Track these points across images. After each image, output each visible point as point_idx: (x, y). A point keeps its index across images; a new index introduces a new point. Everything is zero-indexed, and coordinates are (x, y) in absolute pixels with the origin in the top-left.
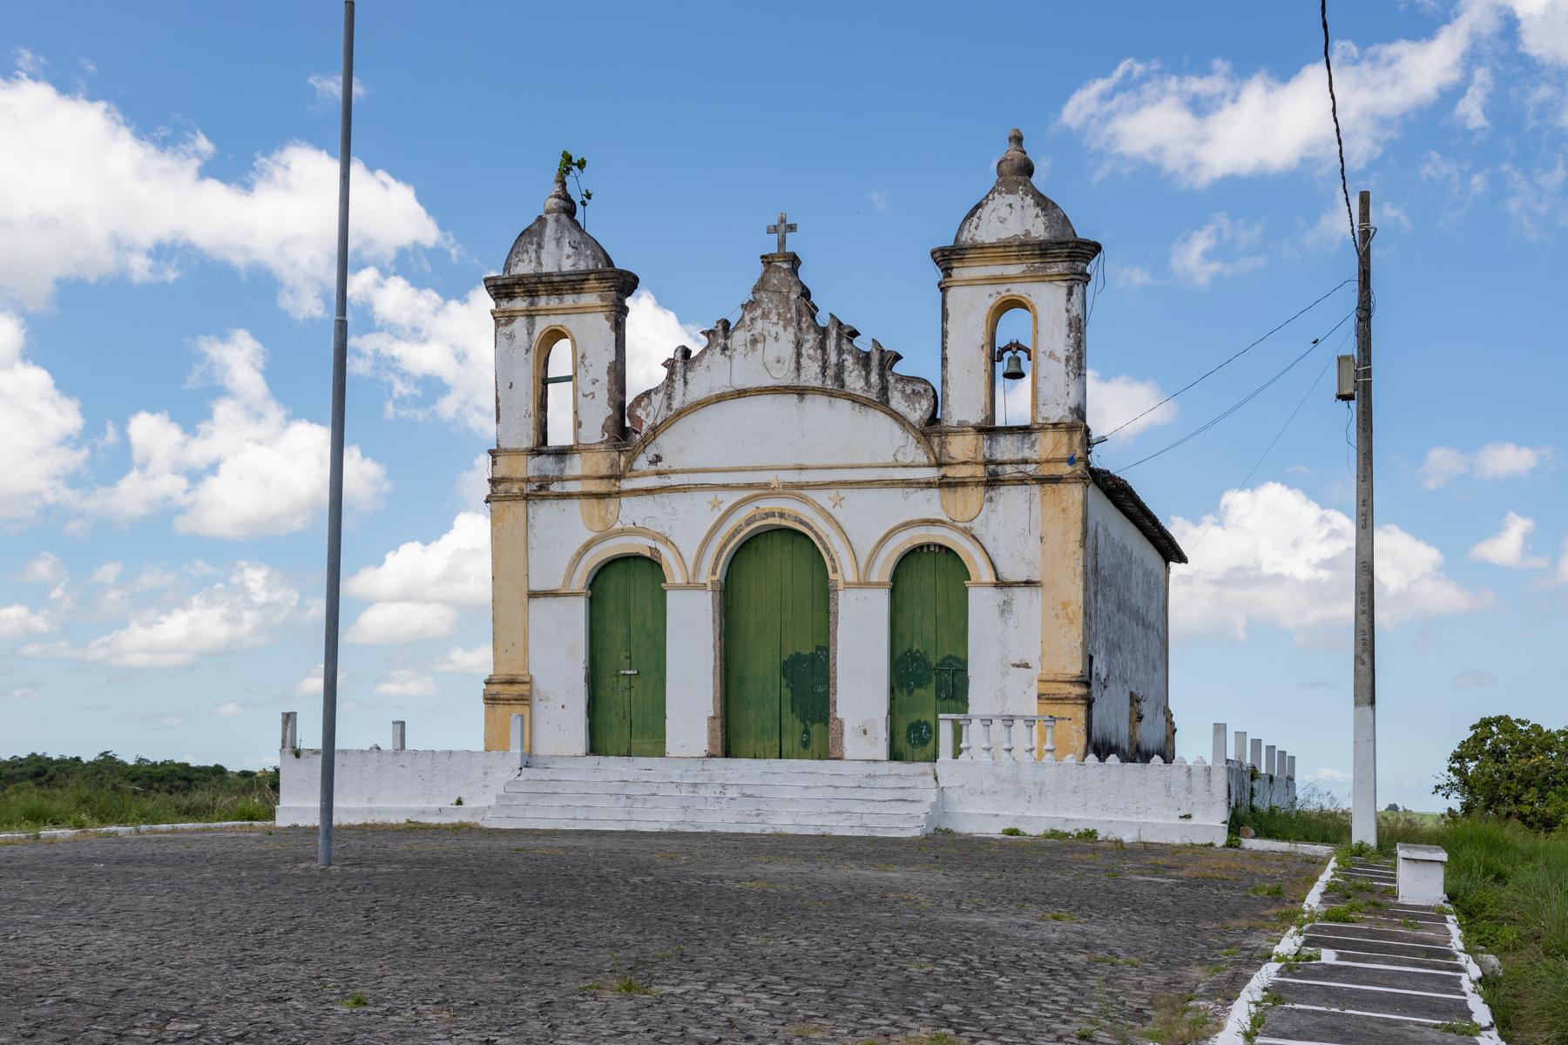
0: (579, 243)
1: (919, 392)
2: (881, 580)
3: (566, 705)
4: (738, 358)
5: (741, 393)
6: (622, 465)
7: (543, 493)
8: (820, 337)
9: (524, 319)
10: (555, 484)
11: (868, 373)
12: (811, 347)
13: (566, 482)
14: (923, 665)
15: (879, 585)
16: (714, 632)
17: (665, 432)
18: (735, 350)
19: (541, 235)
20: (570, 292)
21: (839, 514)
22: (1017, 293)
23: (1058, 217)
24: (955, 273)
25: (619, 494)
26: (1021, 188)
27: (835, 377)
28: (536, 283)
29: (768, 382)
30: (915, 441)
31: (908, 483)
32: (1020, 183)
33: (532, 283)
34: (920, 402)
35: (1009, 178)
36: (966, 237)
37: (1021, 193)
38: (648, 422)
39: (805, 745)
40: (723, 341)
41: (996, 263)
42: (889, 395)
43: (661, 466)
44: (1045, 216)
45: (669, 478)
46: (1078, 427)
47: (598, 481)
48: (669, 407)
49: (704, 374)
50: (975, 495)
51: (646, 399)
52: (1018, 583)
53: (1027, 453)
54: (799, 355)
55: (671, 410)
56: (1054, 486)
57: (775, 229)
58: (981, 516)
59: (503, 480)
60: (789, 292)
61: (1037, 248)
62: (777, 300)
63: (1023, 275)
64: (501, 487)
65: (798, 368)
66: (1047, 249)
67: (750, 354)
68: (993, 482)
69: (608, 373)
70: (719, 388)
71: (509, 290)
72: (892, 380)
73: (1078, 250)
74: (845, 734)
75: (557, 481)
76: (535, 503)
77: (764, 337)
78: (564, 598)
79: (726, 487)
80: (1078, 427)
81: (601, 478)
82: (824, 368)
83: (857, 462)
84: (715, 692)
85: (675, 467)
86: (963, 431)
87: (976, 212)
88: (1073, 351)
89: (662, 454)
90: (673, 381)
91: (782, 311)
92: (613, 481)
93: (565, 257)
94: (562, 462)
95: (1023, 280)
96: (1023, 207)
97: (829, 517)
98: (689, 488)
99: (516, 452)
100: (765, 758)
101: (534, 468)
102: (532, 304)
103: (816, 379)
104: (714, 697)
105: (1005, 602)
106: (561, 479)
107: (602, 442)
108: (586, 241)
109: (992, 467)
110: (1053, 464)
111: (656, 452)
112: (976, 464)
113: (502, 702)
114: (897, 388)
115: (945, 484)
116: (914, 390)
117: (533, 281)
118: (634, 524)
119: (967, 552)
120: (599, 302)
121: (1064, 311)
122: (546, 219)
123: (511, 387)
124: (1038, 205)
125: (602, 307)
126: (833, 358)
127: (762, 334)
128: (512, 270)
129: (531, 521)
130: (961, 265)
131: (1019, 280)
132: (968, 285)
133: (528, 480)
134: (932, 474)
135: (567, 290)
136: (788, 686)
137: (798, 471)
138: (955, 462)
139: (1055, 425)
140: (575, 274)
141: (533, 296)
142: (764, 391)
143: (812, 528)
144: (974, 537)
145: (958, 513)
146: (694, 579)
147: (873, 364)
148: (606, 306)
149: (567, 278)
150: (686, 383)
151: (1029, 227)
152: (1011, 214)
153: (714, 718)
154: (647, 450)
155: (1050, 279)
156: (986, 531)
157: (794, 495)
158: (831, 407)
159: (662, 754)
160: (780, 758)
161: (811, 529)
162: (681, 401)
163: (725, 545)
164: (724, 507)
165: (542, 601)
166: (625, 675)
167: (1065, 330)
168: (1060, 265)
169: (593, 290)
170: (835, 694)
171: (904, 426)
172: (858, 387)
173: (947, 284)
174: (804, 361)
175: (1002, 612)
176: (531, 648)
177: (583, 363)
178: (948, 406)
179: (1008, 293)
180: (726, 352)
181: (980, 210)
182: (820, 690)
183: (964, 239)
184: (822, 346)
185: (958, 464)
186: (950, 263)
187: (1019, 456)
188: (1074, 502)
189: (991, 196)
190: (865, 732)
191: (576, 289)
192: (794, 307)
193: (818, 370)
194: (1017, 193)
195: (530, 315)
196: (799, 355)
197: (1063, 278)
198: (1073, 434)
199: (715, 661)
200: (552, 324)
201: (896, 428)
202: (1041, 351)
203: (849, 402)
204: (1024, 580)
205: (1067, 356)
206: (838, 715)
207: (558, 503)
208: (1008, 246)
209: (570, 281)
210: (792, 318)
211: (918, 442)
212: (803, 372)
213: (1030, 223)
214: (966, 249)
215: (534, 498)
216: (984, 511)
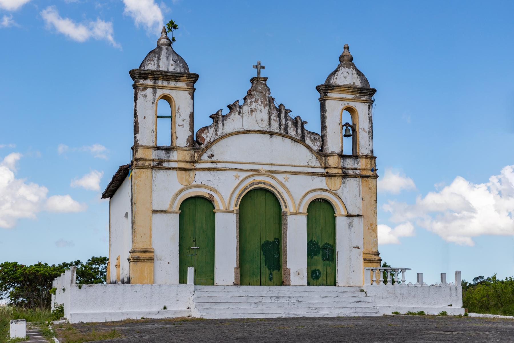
0: (177, 60)
1: (316, 138)
2: (304, 212)
3: (170, 263)
4: (245, 117)
5: (248, 132)
6: (196, 157)
7: (160, 166)
8: (278, 113)
9: (151, 89)
10: (165, 163)
11: (297, 129)
12: (275, 116)
13: (170, 163)
14: (317, 247)
15: (303, 214)
16: (237, 231)
17: (215, 145)
18: (244, 114)
19: (160, 54)
21: (287, 184)
22: (351, 105)
24: (329, 94)
25: (196, 169)
27: (284, 129)
28: (159, 75)
29: (257, 128)
30: (316, 158)
31: (314, 174)
32: (351, 65)
33: (157, 74)
34: (317, 142)
35: (347, 62)
36: (332, 81)
37: (351, 68)
38: (207, 140)
39: (271, 279)
40: (239, 109)
42: (305, 138)
43: (213, 159)
44: (360, 78)
45: (217, 164)
46: (374, 158)
47: (185, 163)
48: (216, 134)
49: (231, 122)
50: (339, 180)
51: (206, 130)
52: (355, 215)
53: (356, 166)
54: (270, 119)
55: (217, 136)
56: (366, 179)
57: (257, 67)
58: (340, 189)
59: (141, 159)
60: (266, 93)
61: (359, 90)
62: (261, 96)
63: (354, 99)
64: (140, 163)
65: (270, 124)
67: (250, 116)
68: (345, 176)
70: (237, 129)
72: (306, 133)
73: (372, 93)
74: (291, 275)
75: (167, 162)
76: (156, 171)
77: (256, 110)
78: (169, 214)
79: (242, 170)
80: (374, 158)
81: (187, 162)
82: (280, 125)
83: (293, 164)
84: (237, 257)
85: (219, 160)
86: (334, 156)
87: (336, 73)
88: (371, 129)
89: (214, 154)
90: (218, 124)
91: (263, 100)
92: (192, 164)
93: (170, 65)
94: (169, 153)
95: (353, 101)
96: (352, 73)
97: (283, 186)
98: (226, 169)
99: (148, 147)
100: (254, 285)
101: (155, 155)
103: (277, 129)
104: (237, 259)
105: (350, 222)
106: (168, 161)
107: (187, 147)
108: (179, 60)
109: (344, 170)
110: (366, 171)
111: (211, 153)
112: (339, 168)
113: (141, 261)
114: (308, 136)
115: (328, 175)
116: (314, 138)
117: (158, 74)
118: (202, 183)
119: (336, 202)
120: (185, 86)
121: (367, 114)
122: (162, 48)
123: (145, 118)
124: (357, 74)
125: (188, 89)
126: (284, 122)
127: (255, 109)
128: (145, 67)
129: (154, 179)
130: (331, 92)
131: (352, 101)
133: (153, 160)
134: (322, 171)
135: (172, 79)
136: (263, 255)
137: (271, 166)
138: (331, 167)
139: (366, 156)
140: (178, 73)
141: (156, 80)
142: (257, 132)
143: (276, 189)
144: (338, 196)
145: (332, 187)
146: (229, 208)
147: (299, 126)
149: (174, 74)
150: (223, 125)
151: (355, 81)
152: (348, 75)
153: (237, 268)
154: (207, 152)
155: (362, 102)
156: (343, 195)
157: (270, 175)
158: (283, 141)
159: (213, 284)
160: (261, 285)
161: (276, 189)
162: (221, 132)
163: (241, 194)
164: (241, 179)
165: (159, 215)
166: (193, 249)
167: (368, 121)
168: (366, 97)
169: (184, 81)
170: (286, 258)
171: (311, 152)
172: (293, 134)
173: (326, 98)
174: (272, 121)
175: (349, 227)
176: (153, 236)
177: (178, 111)
178: (327, 145)
179: (348, 105)
180: (240, 114)
181: (337, 72)
182: (276, 256)
183: (331, 82)
184: (279, 116)
185: (332, 168)
186: (327, 91)
187: (353, 167)
188: (373, 186)
189: (341, 68)
190: (299, 274)
192: (268, 99)
193: (278, 126)
195: (155, 88)
196: (270, 119)
197: (367, 102)
198: (372, 160)
199: (237, 243)
201: (308, 152)
202: (360, 128)
203: (290, 140)
204: (356, 214)
205: (369, 131)
206: (288, 267)
207: (166, 171)
208: (350, 88)
209: (175, 76)
210: (267, 104)
211: (317, 158)
212: (272, 127)
213: (354, 80)
214: (335, 86)
215: (156, 168)
216: (341, 187)
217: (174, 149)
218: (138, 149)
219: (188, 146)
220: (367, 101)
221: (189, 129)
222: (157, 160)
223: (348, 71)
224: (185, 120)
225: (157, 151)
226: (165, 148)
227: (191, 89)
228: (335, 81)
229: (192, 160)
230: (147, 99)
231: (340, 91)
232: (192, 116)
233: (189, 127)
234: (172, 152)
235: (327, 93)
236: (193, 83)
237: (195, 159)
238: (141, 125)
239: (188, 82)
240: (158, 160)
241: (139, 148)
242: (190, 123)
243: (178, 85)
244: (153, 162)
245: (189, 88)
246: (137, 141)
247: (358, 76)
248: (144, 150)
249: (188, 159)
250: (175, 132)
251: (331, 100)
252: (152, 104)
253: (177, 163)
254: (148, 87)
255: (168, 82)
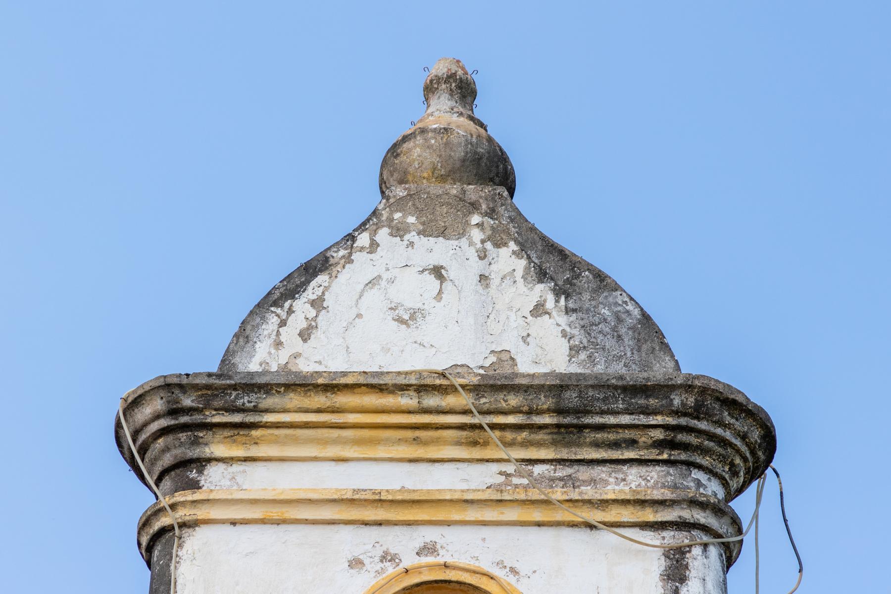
23: (619, 320)
26: (476, 219)
35: (436, 189)
41: (381, 452)
61: (546, 402)
66: (587, 413)
73: (703, 425)
87: (307, 282)
131: (472, 514)
132: (263, 521)
168: (633, 474)
186: (196, 442)
194: (461, 235)
197: (650, 515)
214: (267, 388)
220: (642, 503)
223: (434, 260)
228: (296, 356)
231: (335, 433)
235: (200, 472)
247: (550, 298)
251: (234, 523)
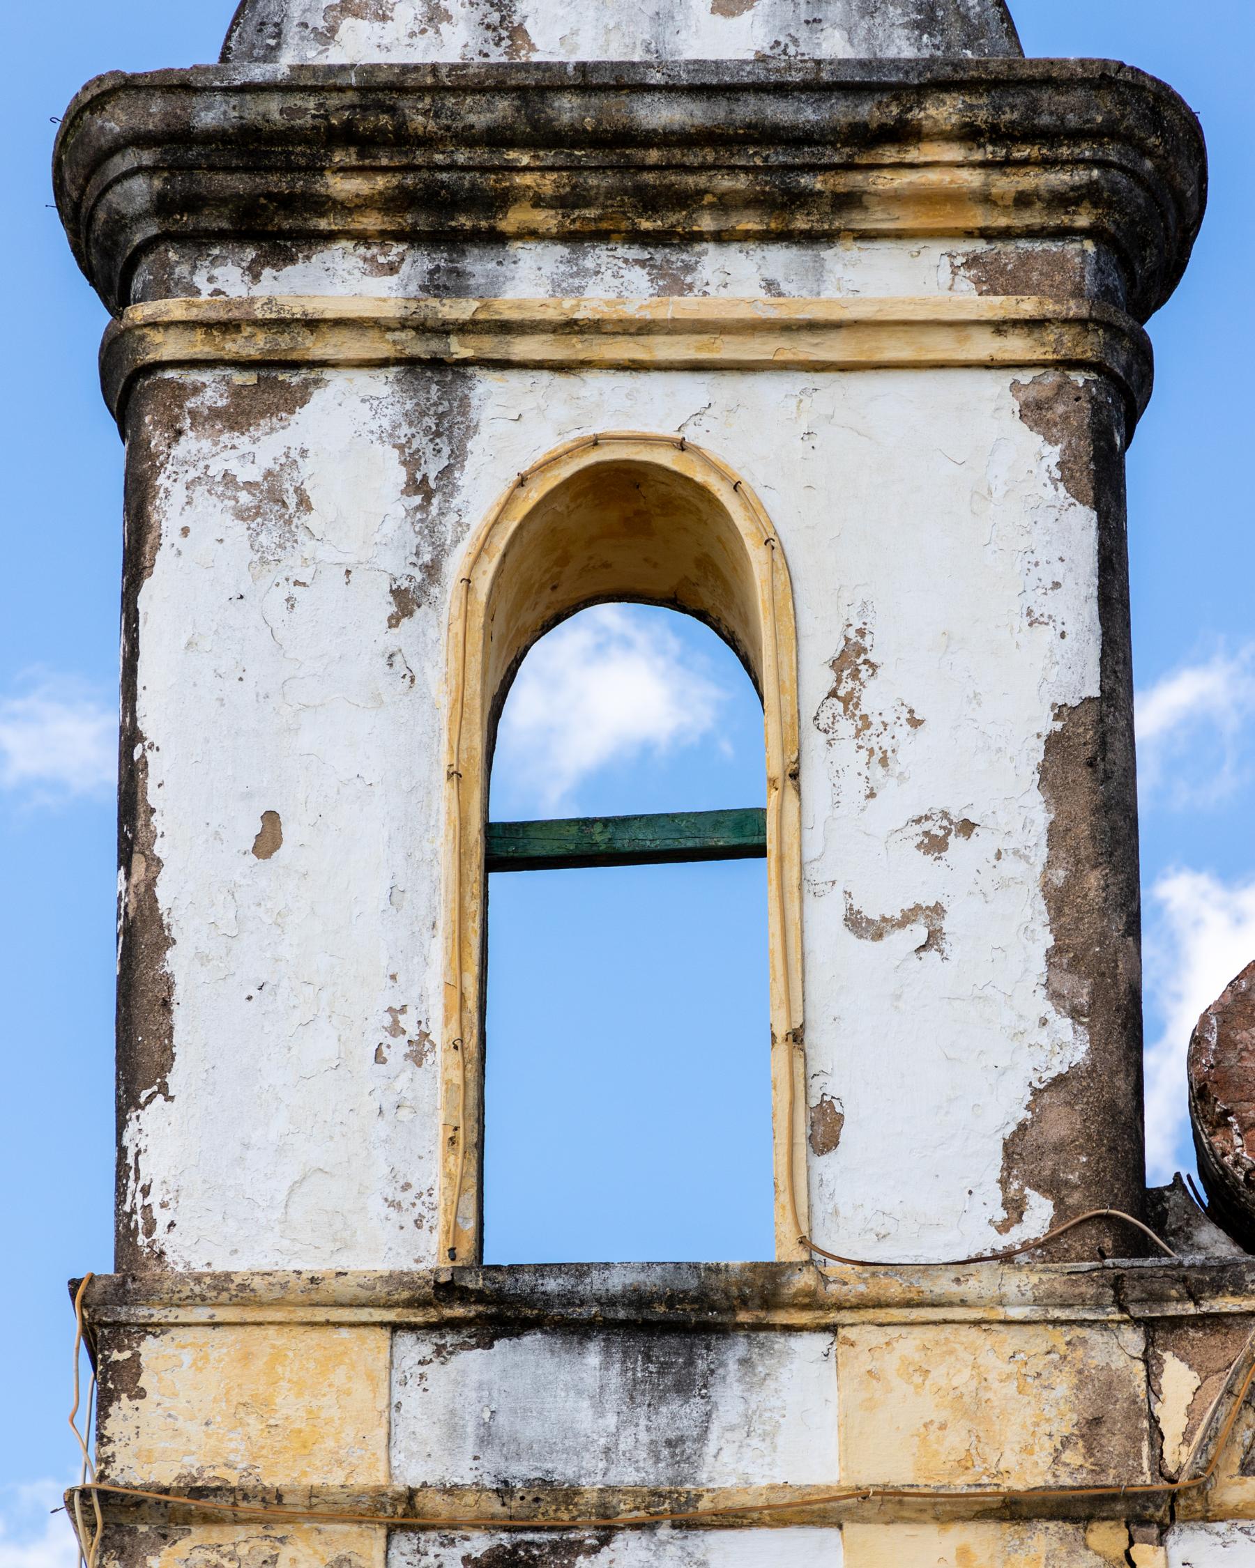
6: (1173, 1420)
9: (381, 384)
20: (749, 222)
69: (1050, 779)
71: (279, 183)
94: (683, 1388)
101: (453, 1430)
102: (434, 286)
107: (1006, 1257)
125: (1000, 327)
135: (724, 204)
148: (1034, 324)
191: (801, 199)
200: (597, 429)
217: (770, 1301)
218: (149, 1348)
219: (1026, 1247)
221: (1040, 966)
222: (467, 1507)
224: (967, 827)
225: (473, 1362)
226: (611, 1301)
227: (1051, 335)
229: (1101, 1469)
230: (308, 547)
232: (1088, 752)
233: (1050, 941)
234: (744, 1362)
236: (1086, 233)
237: (1158, 1460)
238: (203, 959)
239: (1006, 234)
240: (496, 1507)
241: (161, 1328)
242: (1059, 876)
243: (829, 292)
244: (403, 1543)
245: (1028, 307)
246: (147, 1208)
248: (247, 1357)
249: (1043, 1458)
250: (796, 1037)
252: (394, 621)
253: (831, 1534)
254: (317, 348)
255: (659, 255)
